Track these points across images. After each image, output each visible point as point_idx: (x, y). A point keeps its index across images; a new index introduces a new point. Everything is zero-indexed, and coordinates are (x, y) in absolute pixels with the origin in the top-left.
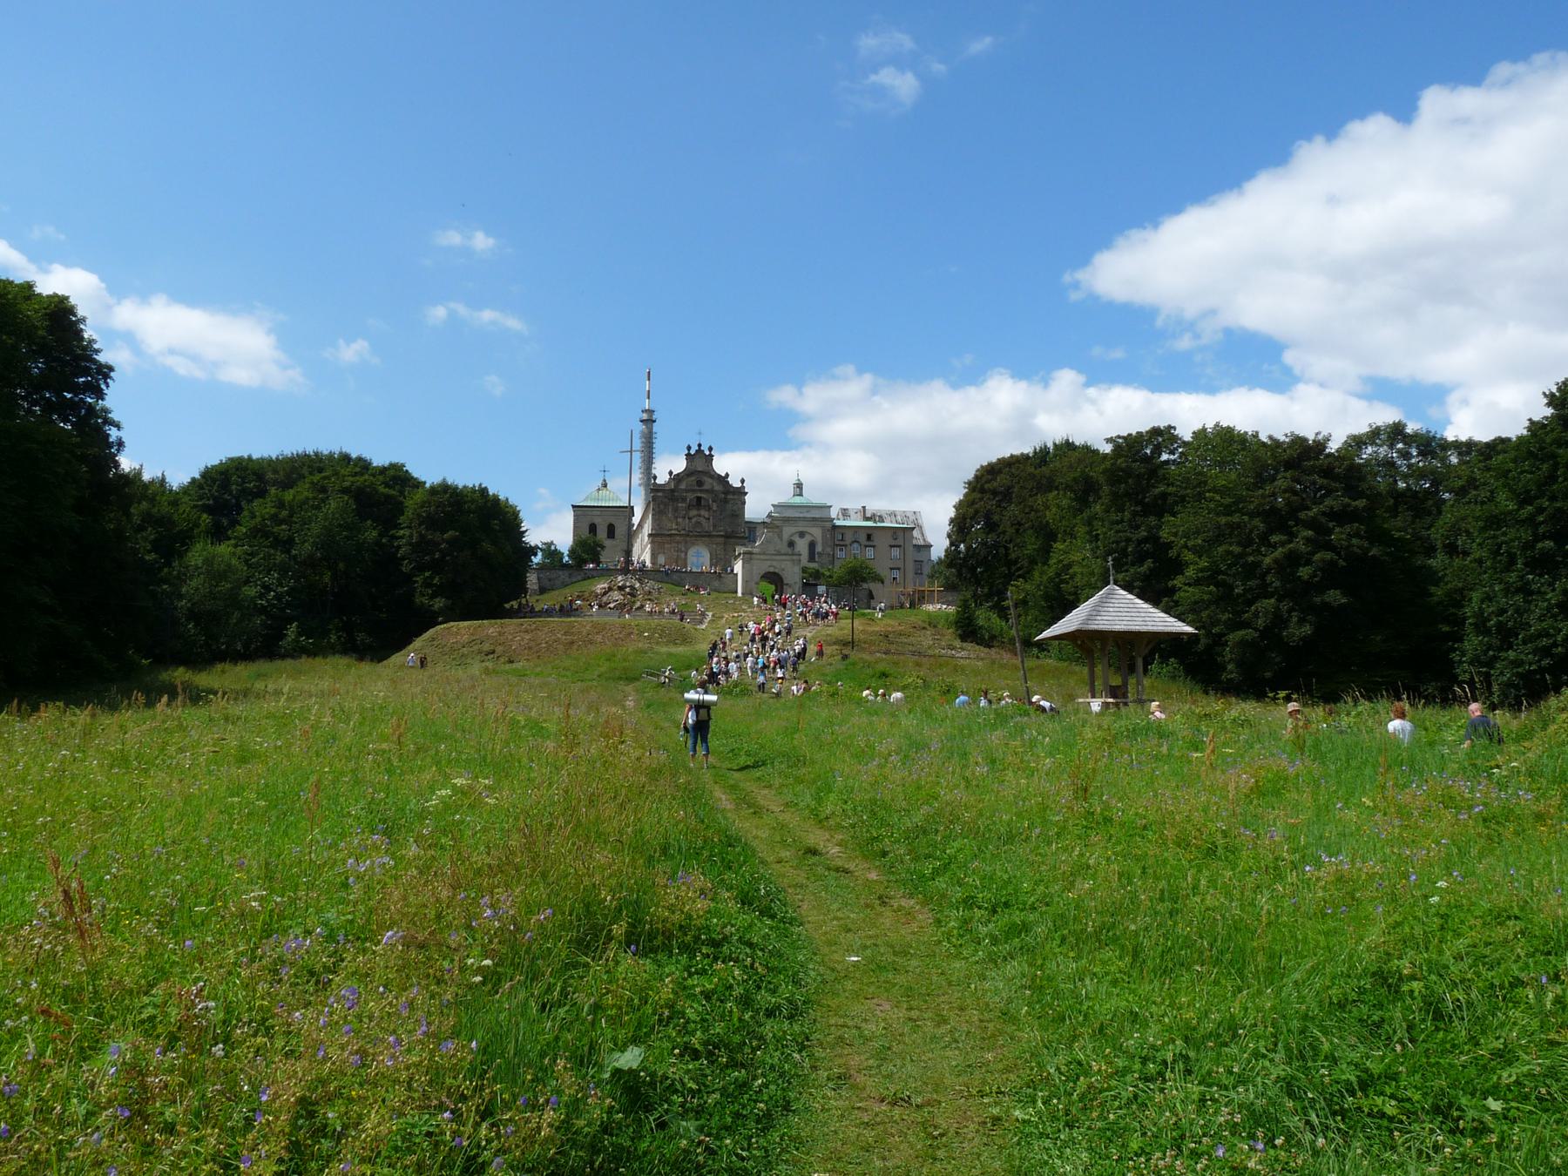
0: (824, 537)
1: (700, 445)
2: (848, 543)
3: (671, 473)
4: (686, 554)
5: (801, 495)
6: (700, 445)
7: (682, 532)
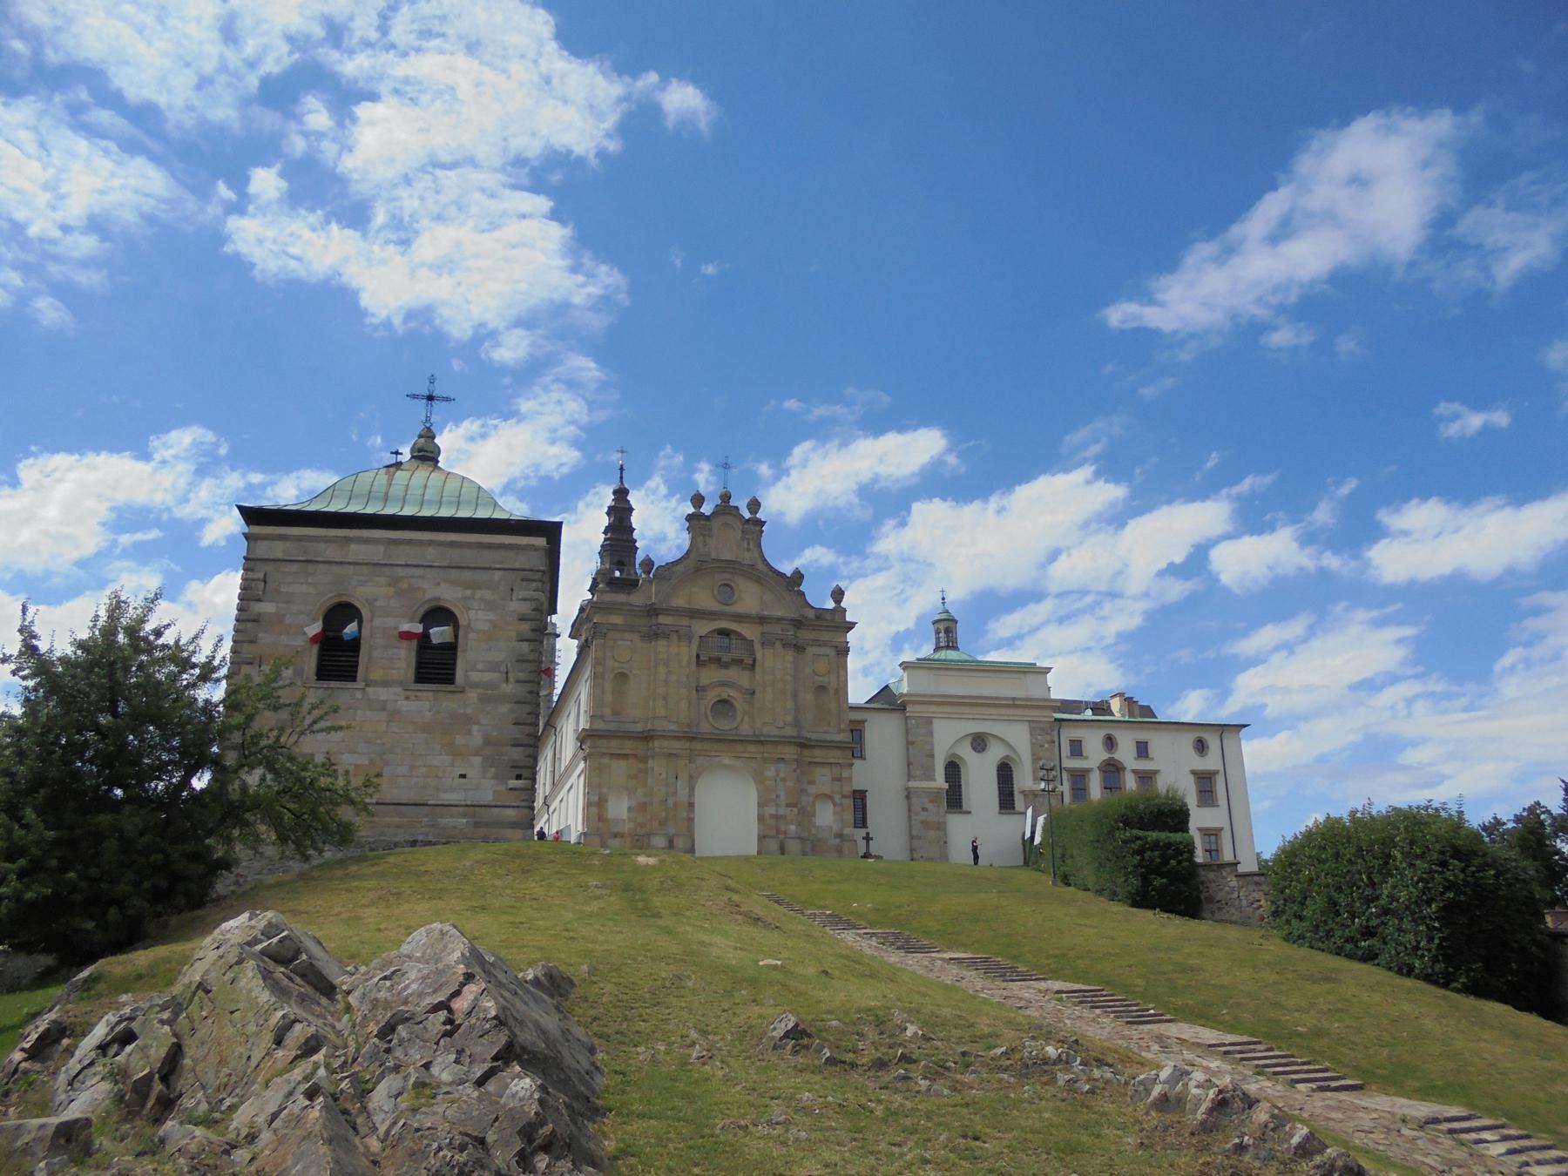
1: (726, 497)
5: (952, 645)
6: (726, 497)
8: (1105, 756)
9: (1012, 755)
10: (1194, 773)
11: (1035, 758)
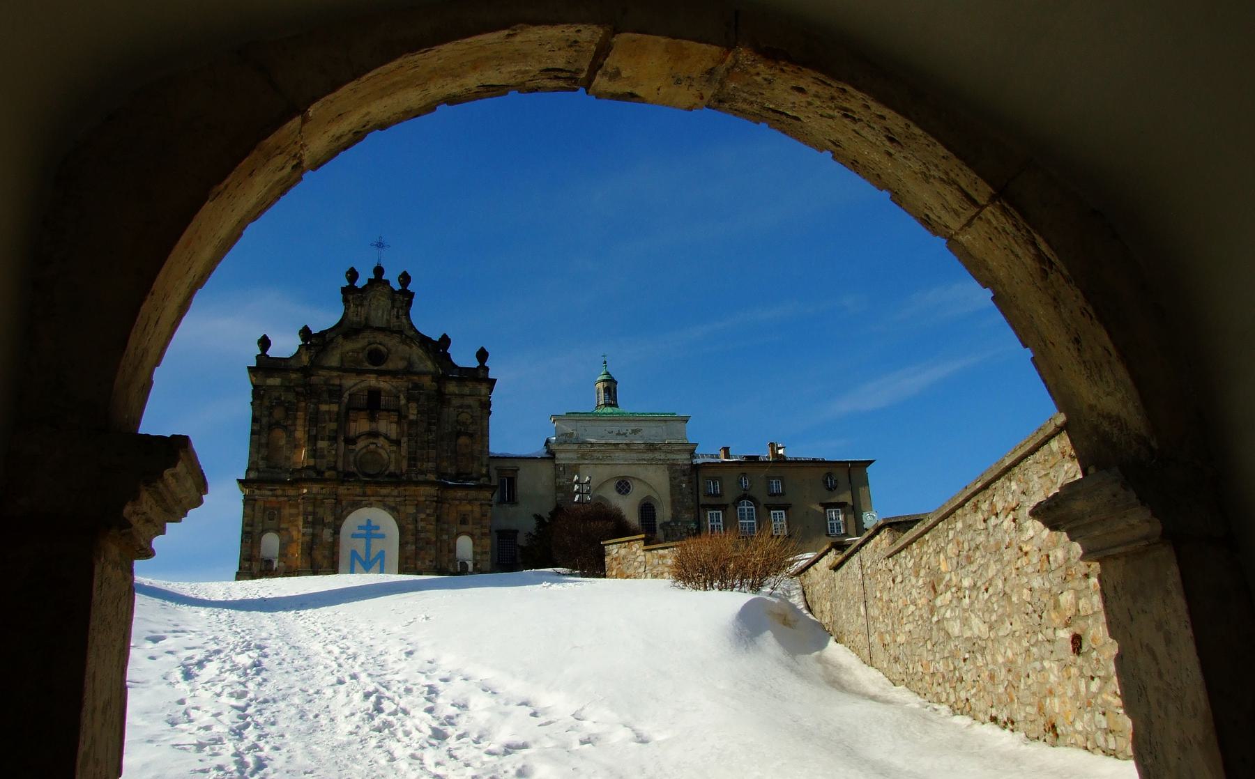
0: (675, 487)
1: (379, 271)
2: (728, 498)
3: (305, 333)
4: (337, 532)
6: (379, 271)
7: (327, 474)
9: (655, 496)
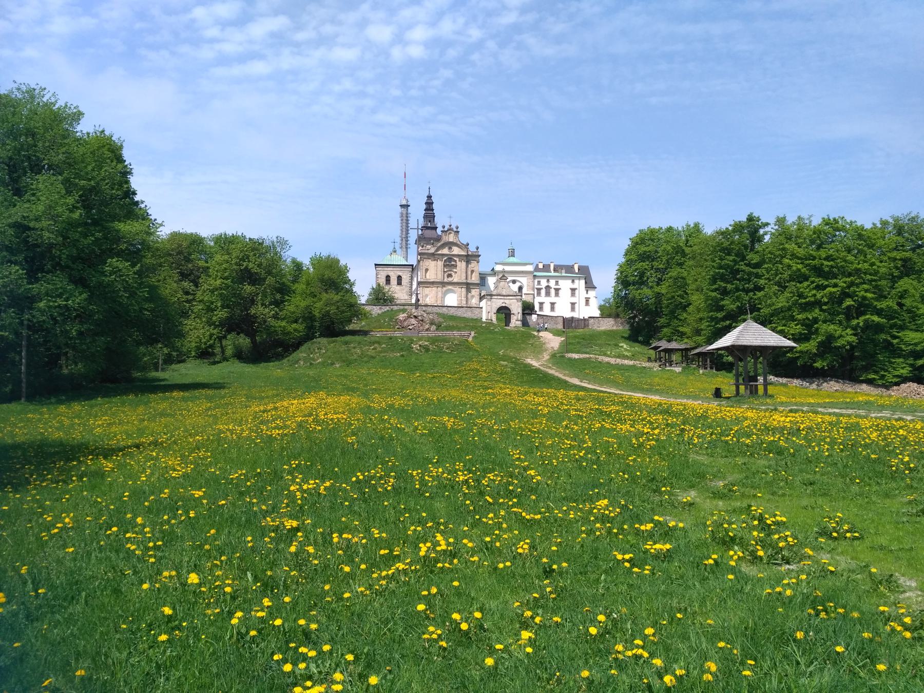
1: (450, 226)
8: (546, 284)
10: (571, 289)
11: (528, 286)
